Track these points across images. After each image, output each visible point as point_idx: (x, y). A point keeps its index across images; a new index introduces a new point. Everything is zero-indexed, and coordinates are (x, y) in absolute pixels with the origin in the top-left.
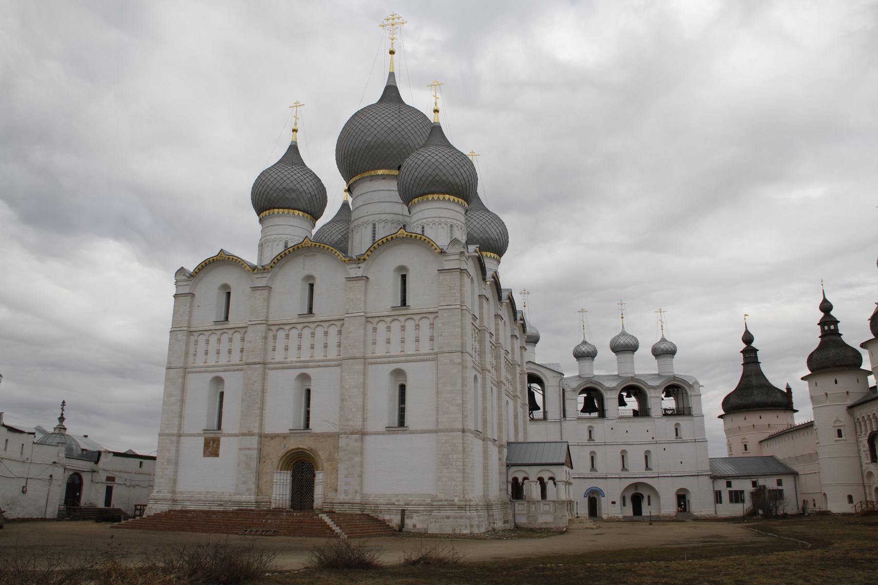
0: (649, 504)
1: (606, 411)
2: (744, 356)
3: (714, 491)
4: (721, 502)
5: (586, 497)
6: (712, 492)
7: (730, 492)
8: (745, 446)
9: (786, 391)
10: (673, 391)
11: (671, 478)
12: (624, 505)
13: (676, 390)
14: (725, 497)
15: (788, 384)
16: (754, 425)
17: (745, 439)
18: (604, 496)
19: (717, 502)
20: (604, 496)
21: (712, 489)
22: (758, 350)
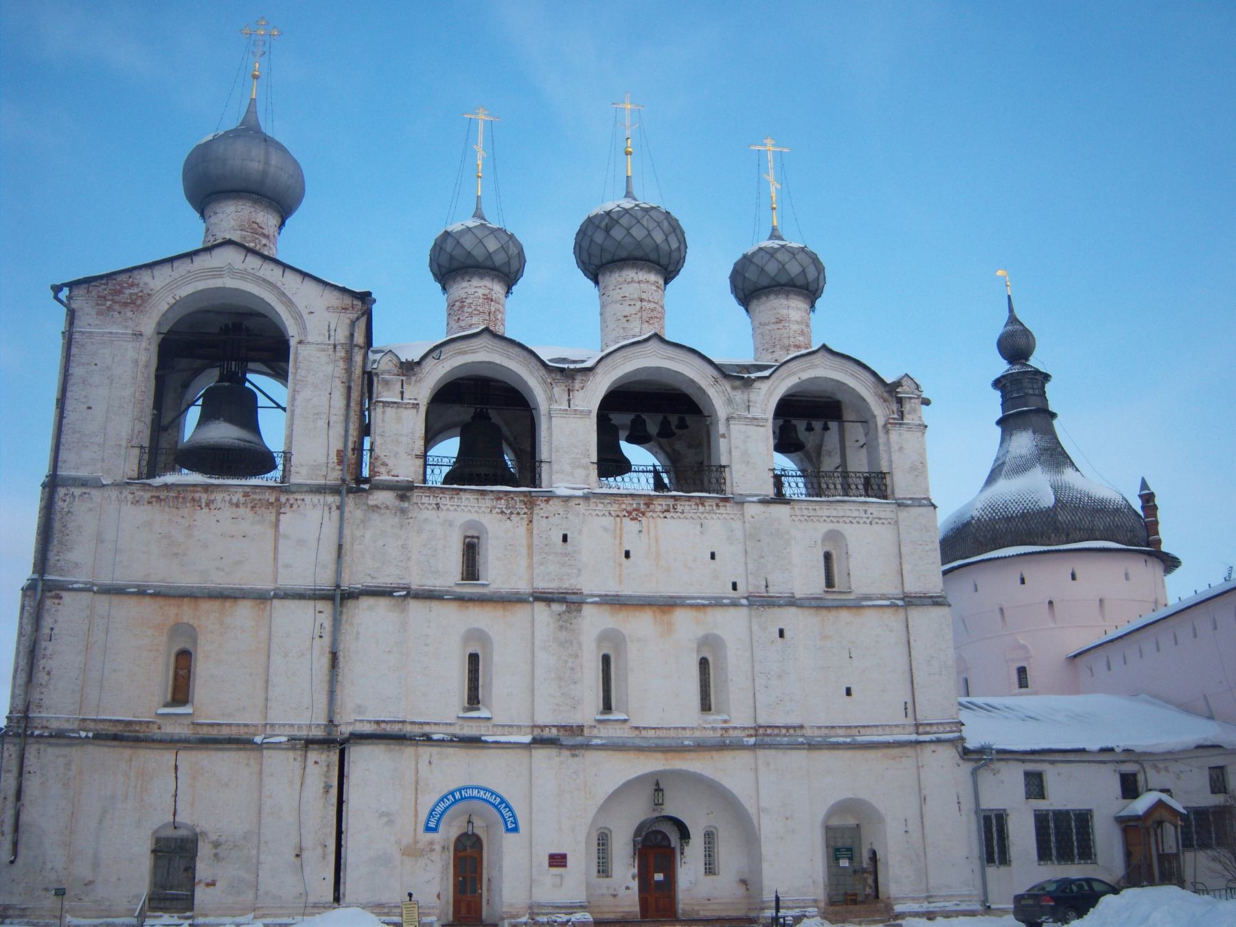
0: (710, 869)
1: (544, 467)
2: (1002, 397)
3: (978, 810)
4: (1004, 860)
5: (435, 830)
6: (973, 817)
7: (1041, 820)
8: (1022, 671)
9: (1137, 505)
10: (810, 429)
11: (804, 753)
12: (604, 870)
13: (817, 425)
14: (1022, 835)
15: (1144, 485)
16: (1051, 603)
17: (1024, 647)
18: (515, 830)
19: (990, 860)
20: (515, 830)
21: (968, 805)
22: (1046, 377)
